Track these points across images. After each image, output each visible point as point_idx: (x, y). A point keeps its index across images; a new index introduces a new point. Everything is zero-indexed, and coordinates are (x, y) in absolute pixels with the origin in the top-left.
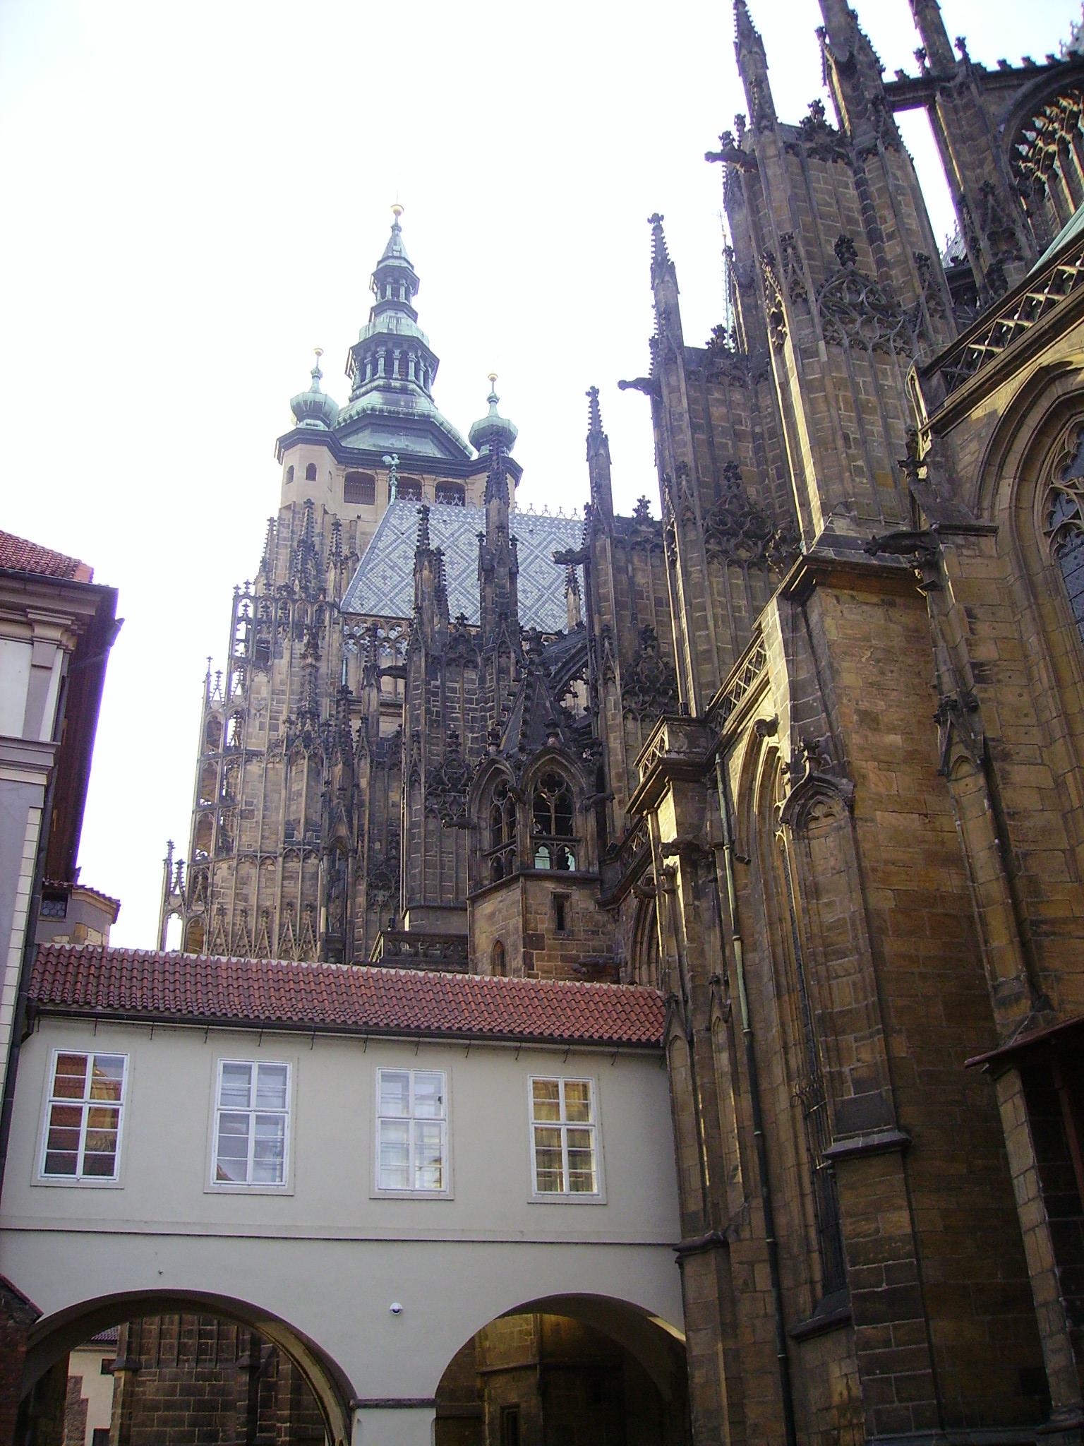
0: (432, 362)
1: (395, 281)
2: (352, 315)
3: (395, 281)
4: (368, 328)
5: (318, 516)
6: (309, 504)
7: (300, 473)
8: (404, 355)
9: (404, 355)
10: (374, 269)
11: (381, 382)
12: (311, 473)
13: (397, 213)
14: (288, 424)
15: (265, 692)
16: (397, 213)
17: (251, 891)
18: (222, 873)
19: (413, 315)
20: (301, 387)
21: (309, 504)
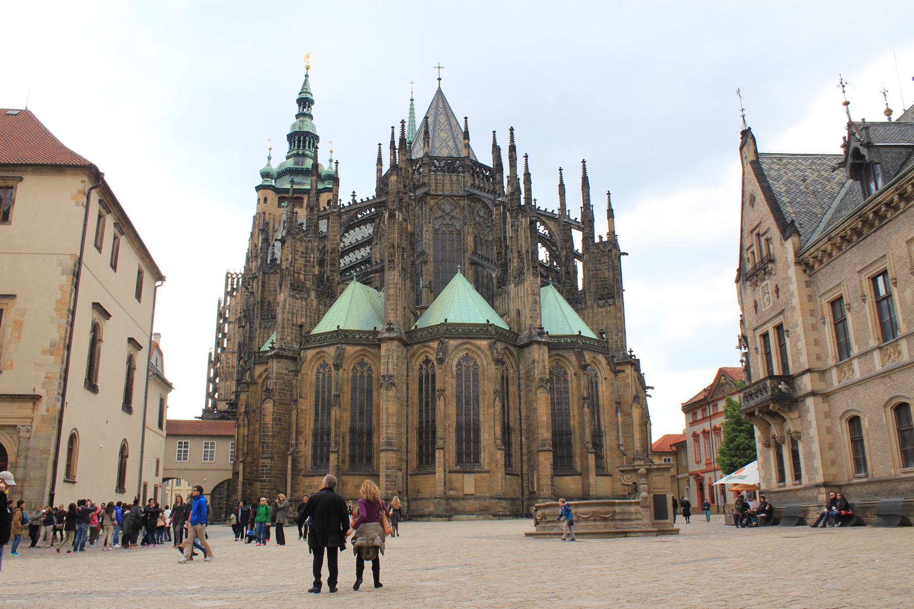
0: (316, 138)
1: (305, 102)
2: (288, 121)
3: (305, 102)
4: (294, 125)
5: (267, 216)
6: (264, 213)
7: (262, 201)
8: (304, 138)
9: (304, 138)
10: (297, 97)
11: (295, 152)
12: (265, 199)
13: (308, 69)
14: (259, 181)
15: (234, 303)
16: (308, 69)
17: (230, 361)
18: (223, 356)
19: (311, 117)
20: (263, 165)
21: (264, 213)
